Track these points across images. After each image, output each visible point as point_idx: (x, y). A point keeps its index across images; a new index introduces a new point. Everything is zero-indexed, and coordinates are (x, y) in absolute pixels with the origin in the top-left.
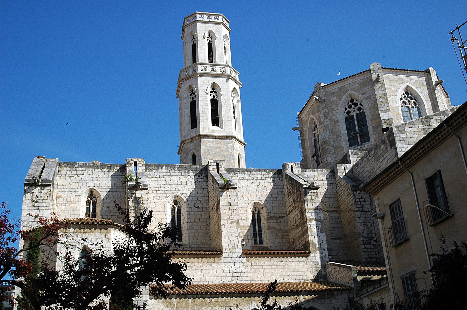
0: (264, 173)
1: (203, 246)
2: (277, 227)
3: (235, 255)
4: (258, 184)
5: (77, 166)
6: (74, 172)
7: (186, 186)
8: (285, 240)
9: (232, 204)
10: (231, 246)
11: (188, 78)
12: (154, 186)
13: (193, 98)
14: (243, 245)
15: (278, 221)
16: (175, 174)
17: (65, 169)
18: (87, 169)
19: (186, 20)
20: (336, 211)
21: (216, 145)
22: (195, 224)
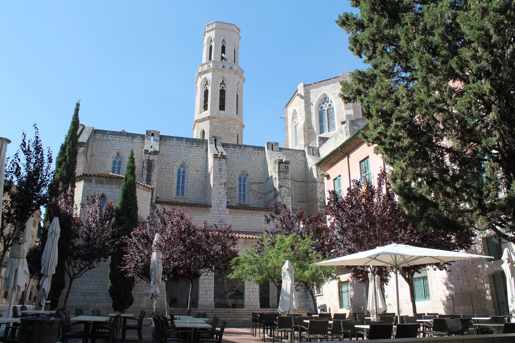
0: (251, 149)
1: (200, 200)
2: (257, 190)
3: (221, 209)
4: (245, 156)
5: (108, 133)
6: (105, 138)
7: (190, 155)
8: (262, 201)
10: (218, 202)
12: (166, 152)
14: (228, 202)
15: (258, 186)
16: (182, 145)
17: (99, 135)
18: (116, 136)
20: (303, 182)
21: (221, 125)
22: (195, 183)
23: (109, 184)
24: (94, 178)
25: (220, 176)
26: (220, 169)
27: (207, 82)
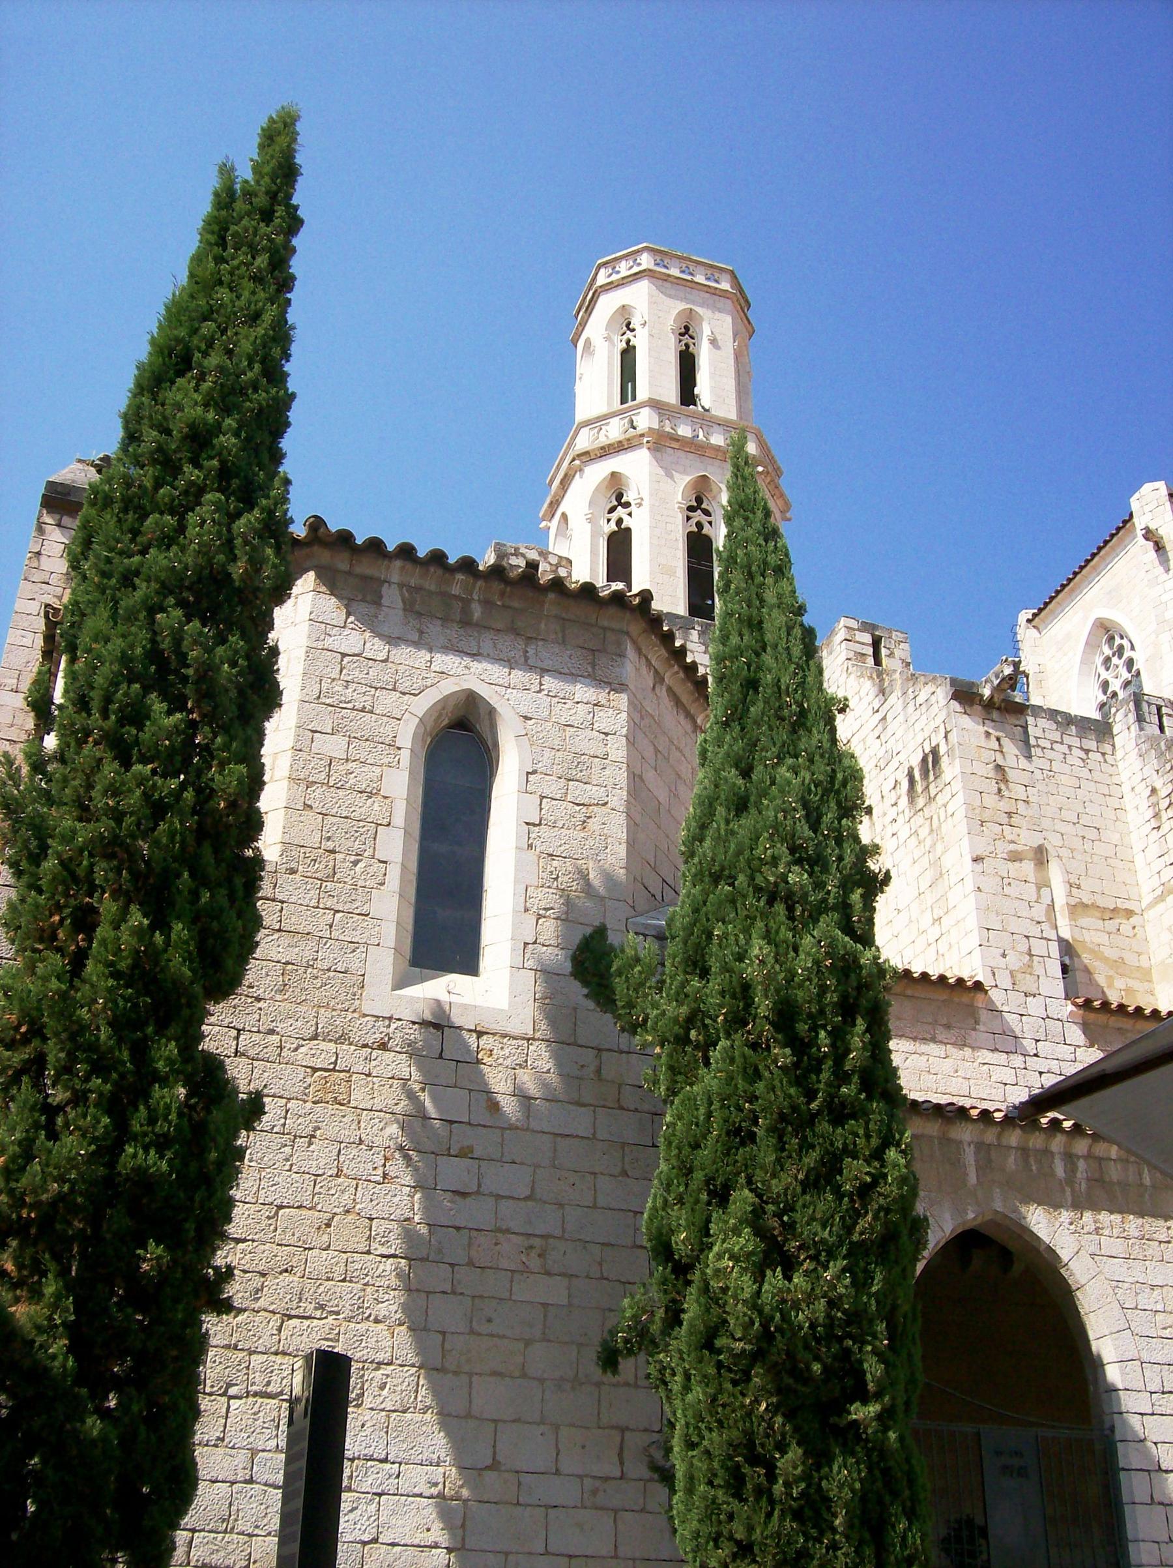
2: (1107, 952)
3: (1035, 1006)
9: (1011, 775)
11: (606, 451)
13: (619, 522)
15: (1111, 925)
19: (602, 271)
23: (515, 631)
24: (395, 571)
25: (1005, 805)
26: (999, 768)
27: (619, 496)
